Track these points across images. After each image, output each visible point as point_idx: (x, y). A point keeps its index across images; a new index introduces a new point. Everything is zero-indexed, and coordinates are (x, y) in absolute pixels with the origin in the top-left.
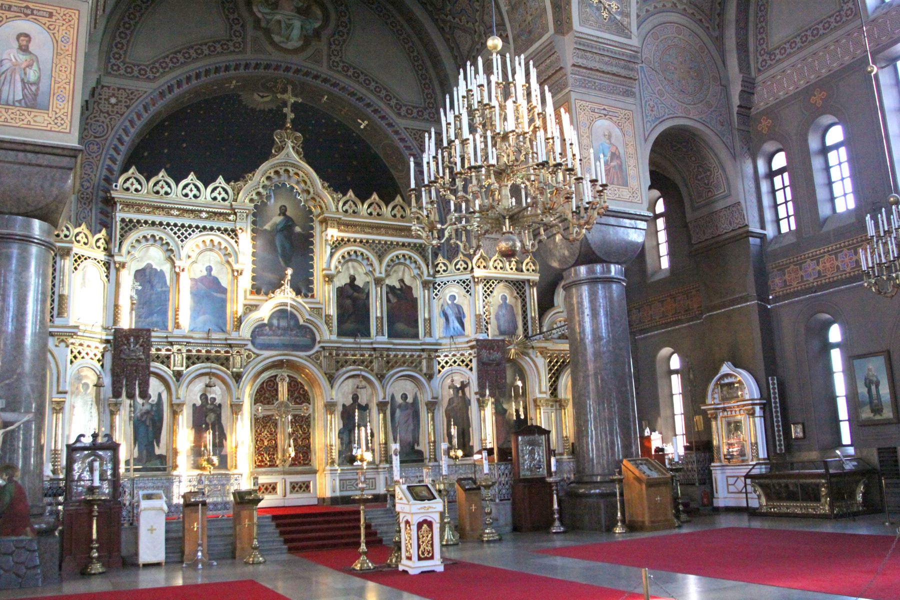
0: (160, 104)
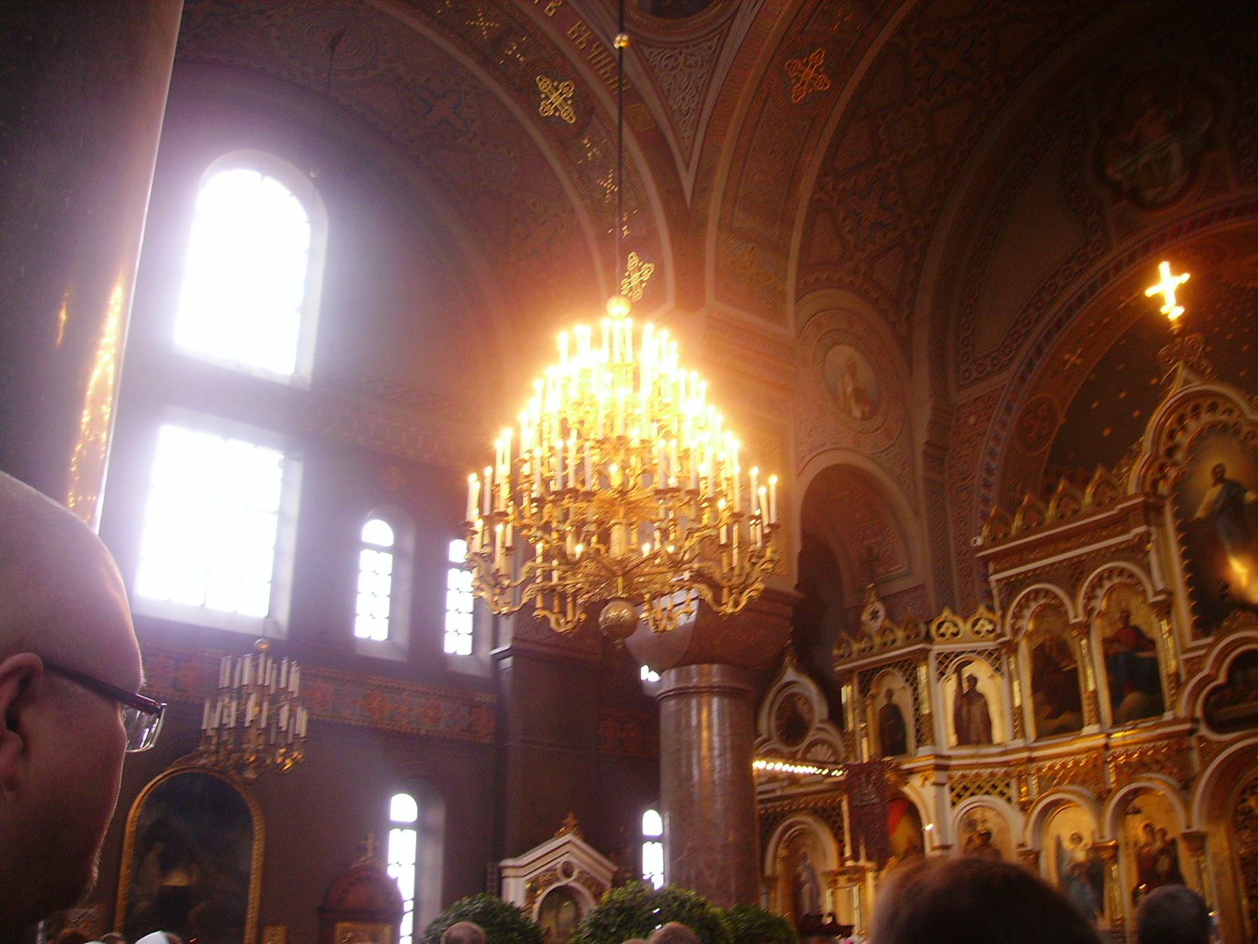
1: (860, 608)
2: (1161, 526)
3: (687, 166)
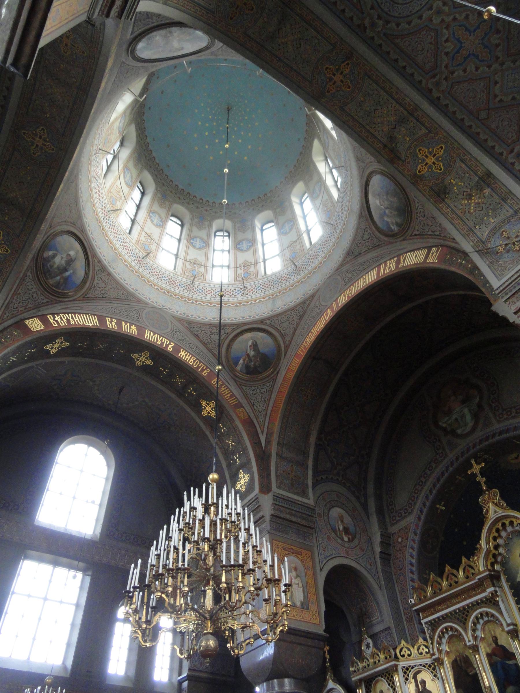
0: (421, 524)
1: (360, 643)
2: (501, 587)
3: (263, 432)
